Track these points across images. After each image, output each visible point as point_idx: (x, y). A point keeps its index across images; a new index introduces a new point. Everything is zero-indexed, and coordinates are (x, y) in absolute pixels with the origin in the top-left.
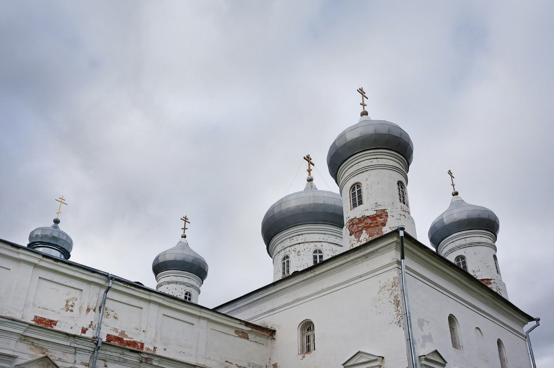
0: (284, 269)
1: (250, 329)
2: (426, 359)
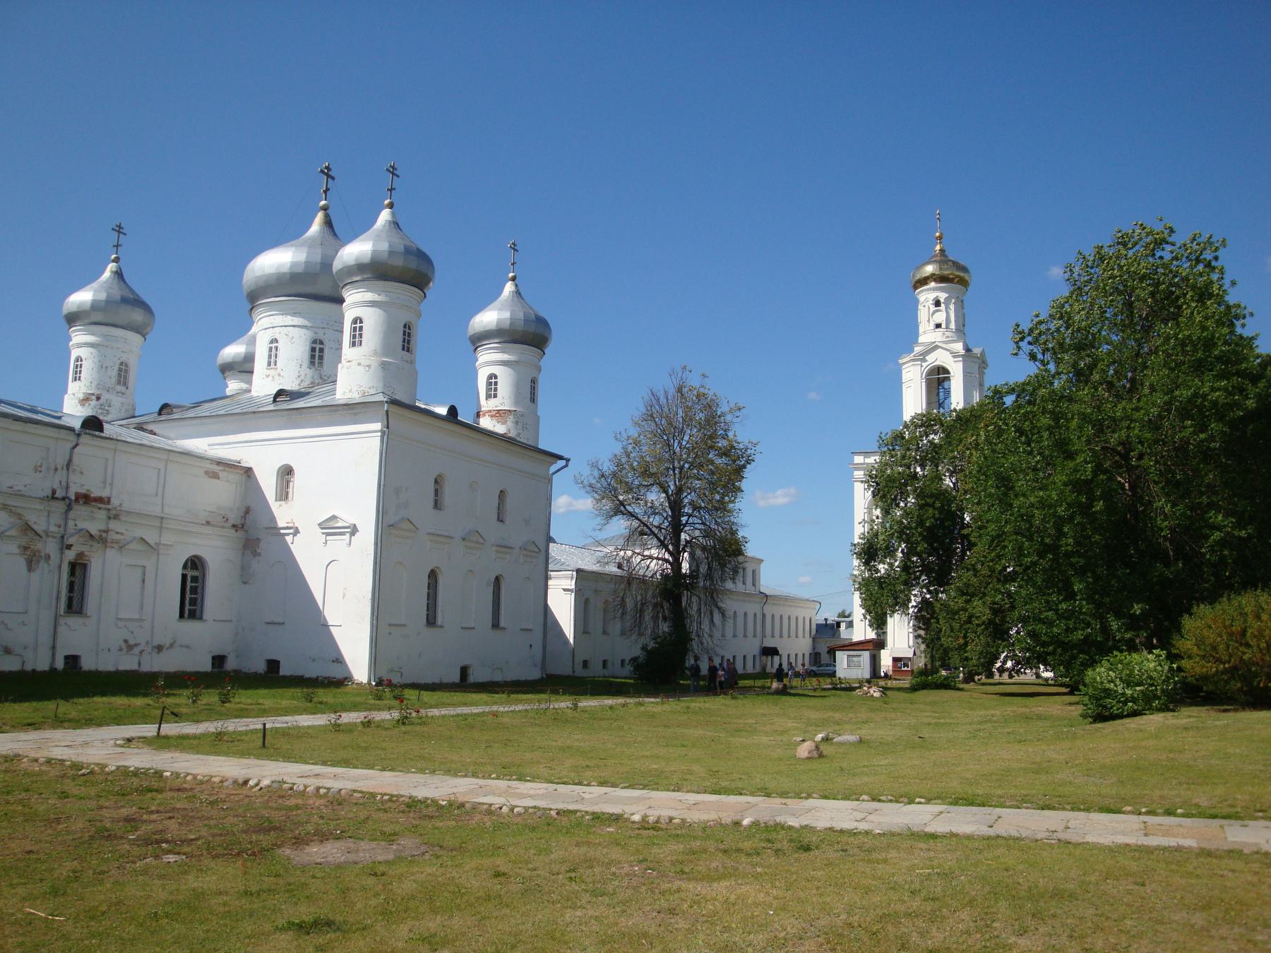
0: (270, 357)
1: (222, 468)
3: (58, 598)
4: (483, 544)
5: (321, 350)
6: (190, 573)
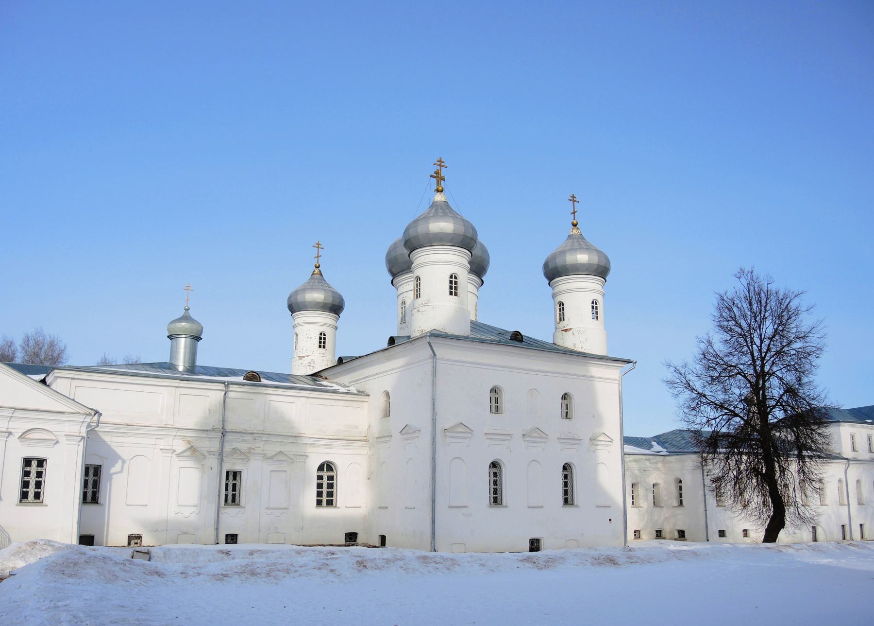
3: (219, 496)
4: (546, 438)
6: (325, 474)
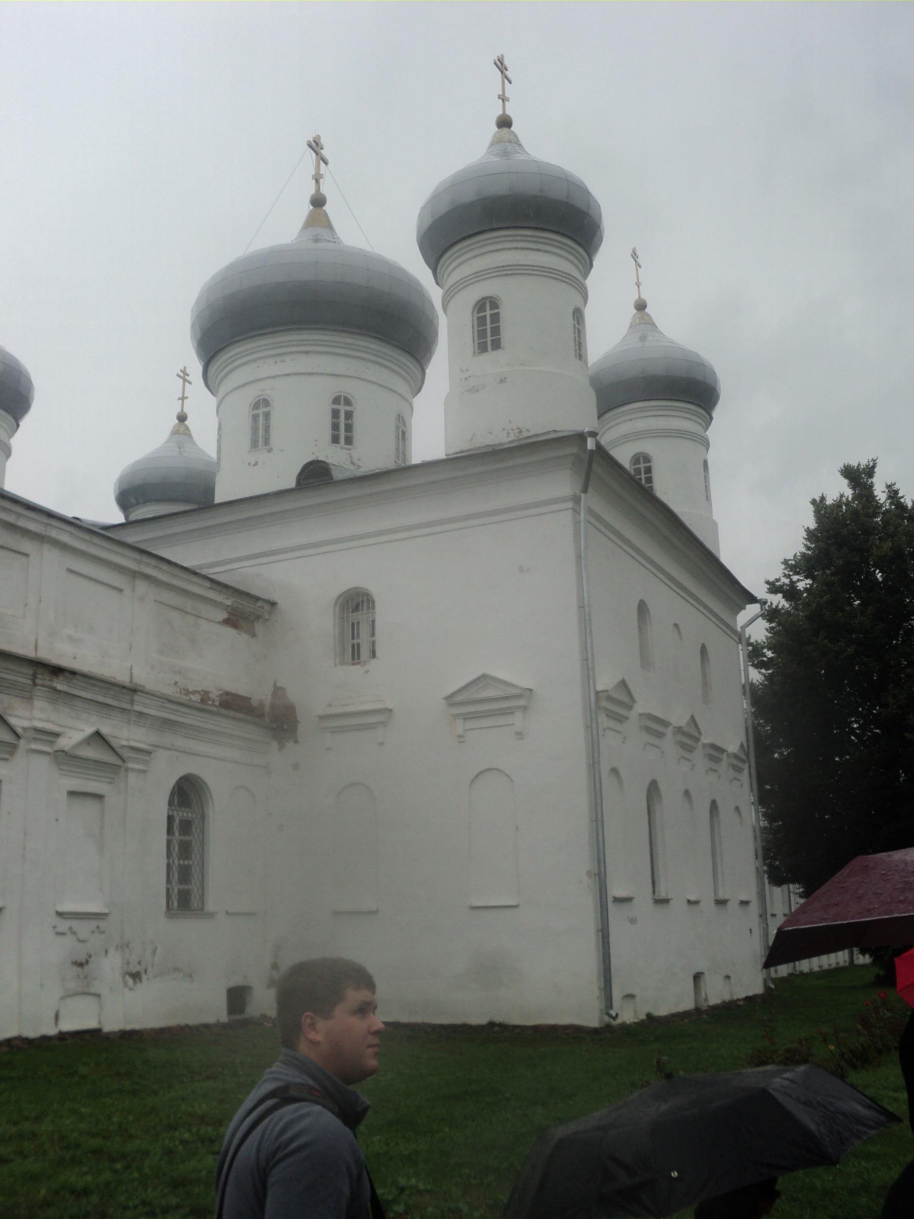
2: (610, 699)
5: (349, 415)
6: (179, 815)
